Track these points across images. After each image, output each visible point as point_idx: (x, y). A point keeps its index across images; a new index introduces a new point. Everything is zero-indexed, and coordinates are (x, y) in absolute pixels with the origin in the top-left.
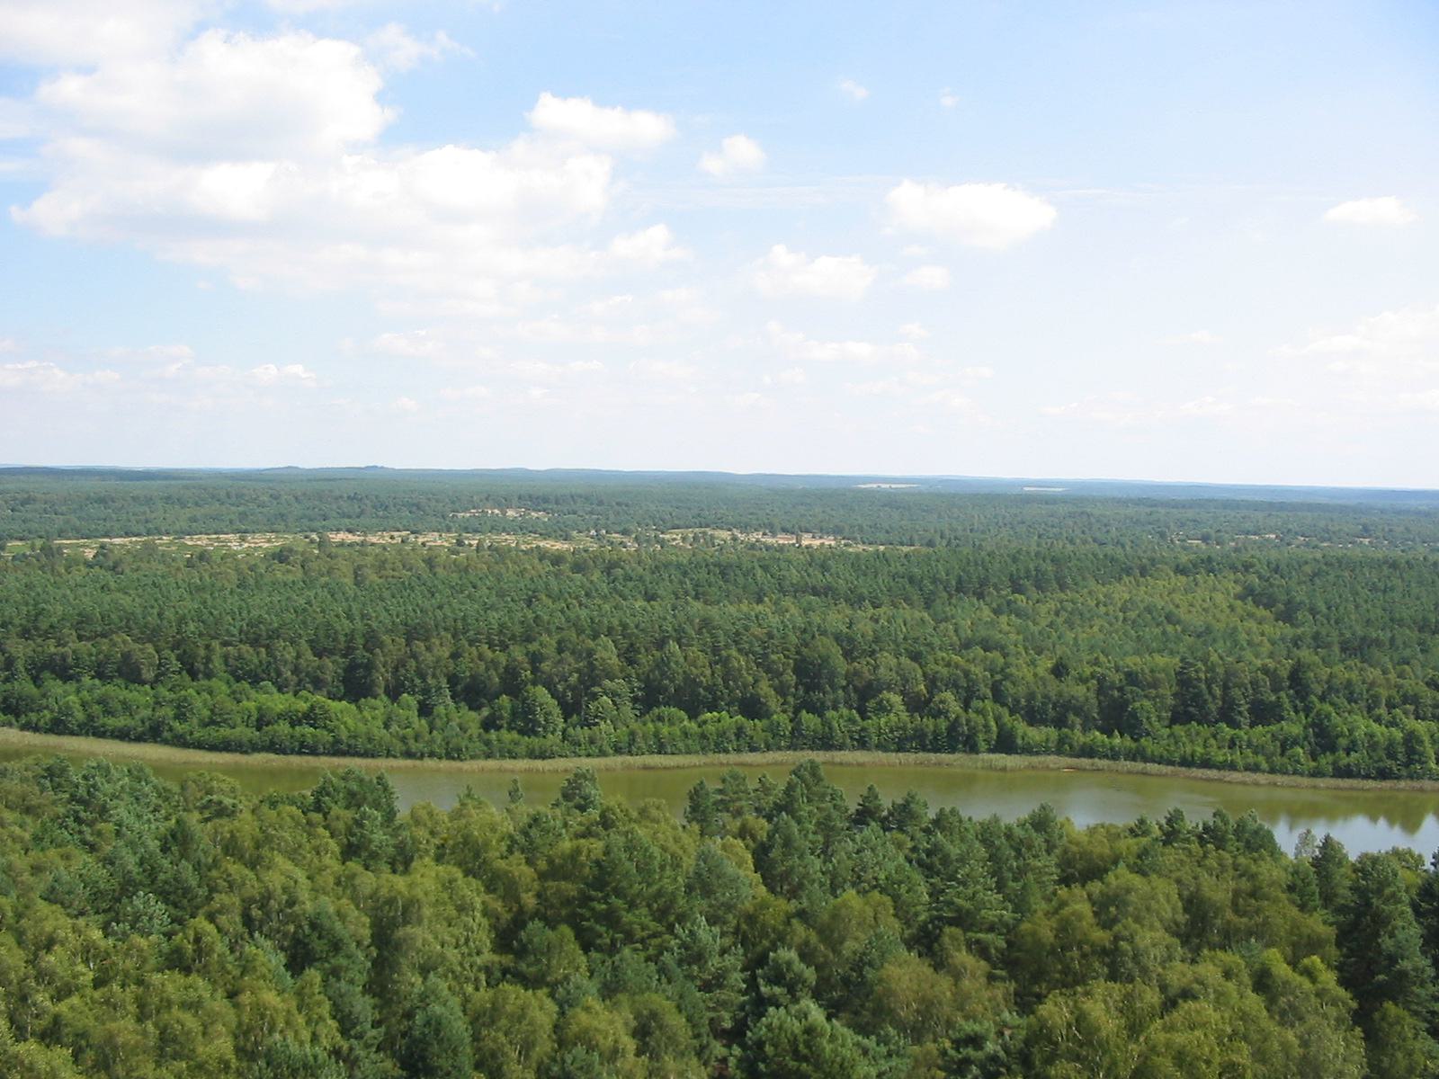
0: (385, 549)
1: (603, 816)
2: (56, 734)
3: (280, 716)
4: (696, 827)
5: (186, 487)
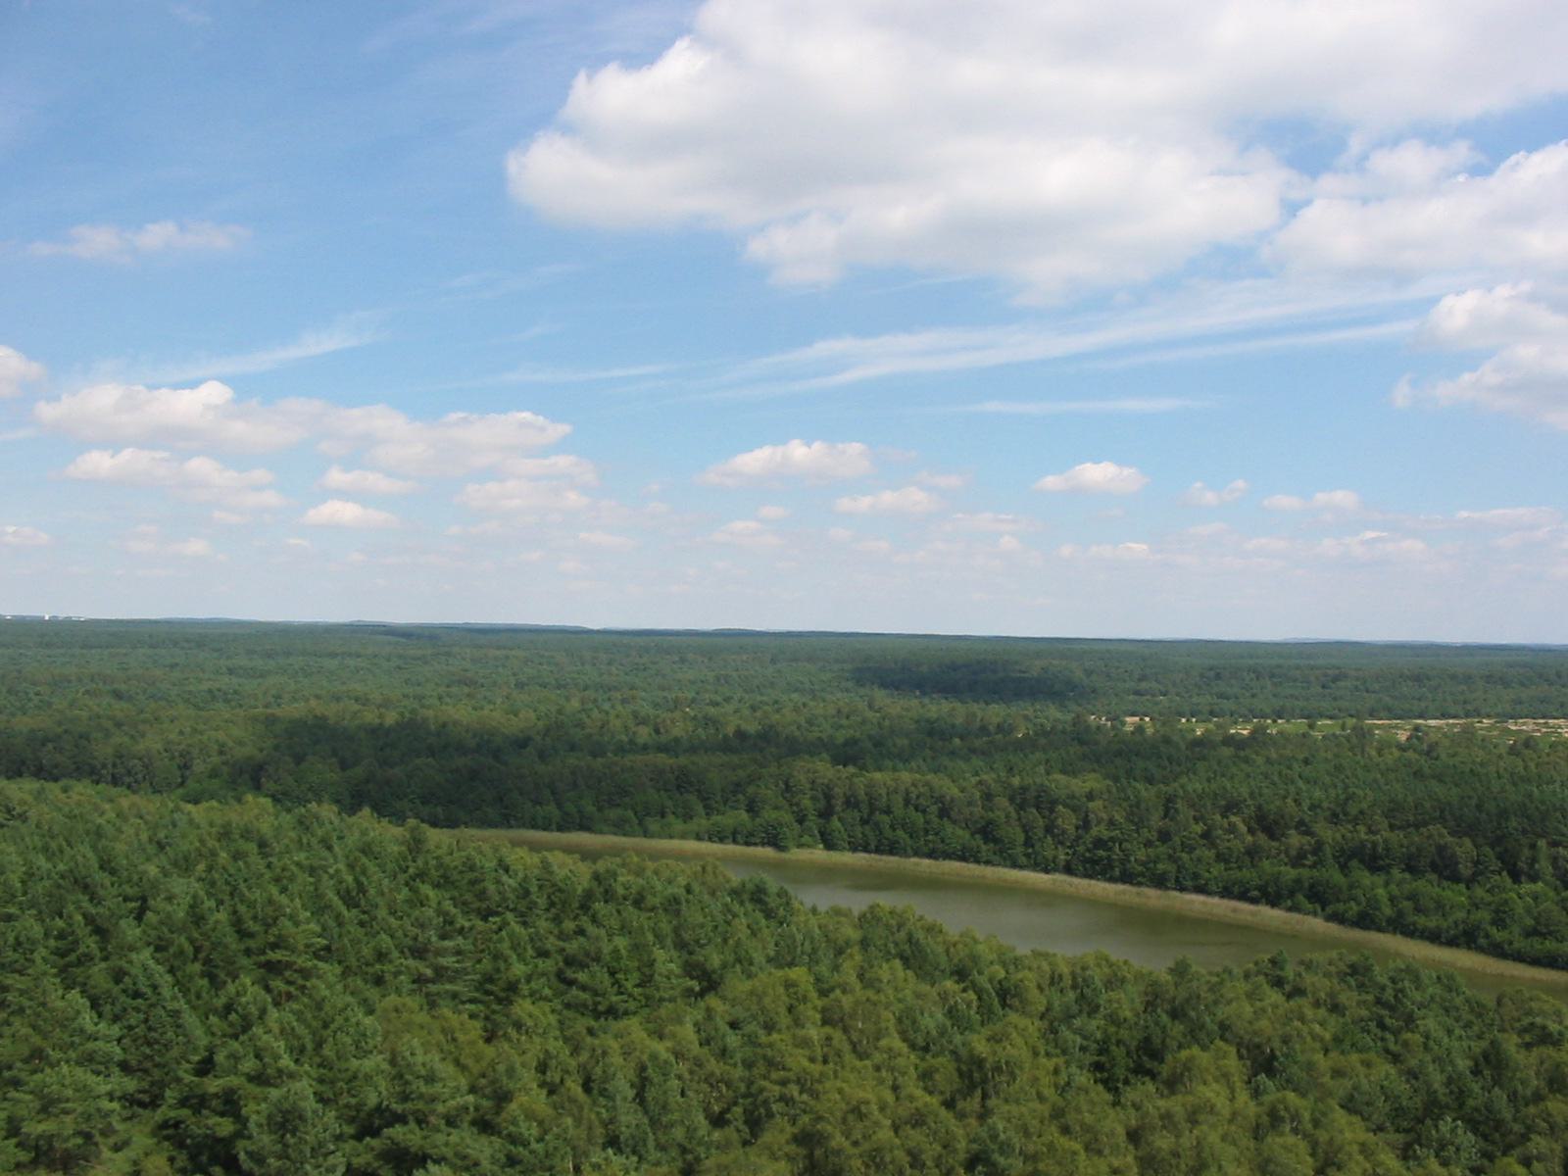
2: (1362, 928)
5: (1511, 666)
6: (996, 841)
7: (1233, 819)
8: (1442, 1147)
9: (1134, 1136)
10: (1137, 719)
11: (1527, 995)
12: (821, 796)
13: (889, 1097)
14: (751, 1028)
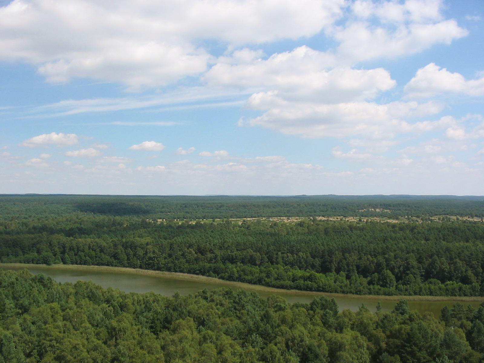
0: (335, 222)
1: (410, 317)
3: (301, 277)
4: (444, 323)
5: (270, 202)
6: (118, 259)
7: (190, 249)
8: (253, 343)
9: (163, 348)
10: (161, 220)
11: (276, 297)
12: (62, 247)
13: (86, 342)
14: (40, 323)
